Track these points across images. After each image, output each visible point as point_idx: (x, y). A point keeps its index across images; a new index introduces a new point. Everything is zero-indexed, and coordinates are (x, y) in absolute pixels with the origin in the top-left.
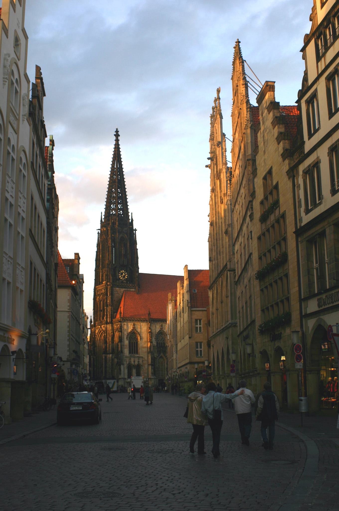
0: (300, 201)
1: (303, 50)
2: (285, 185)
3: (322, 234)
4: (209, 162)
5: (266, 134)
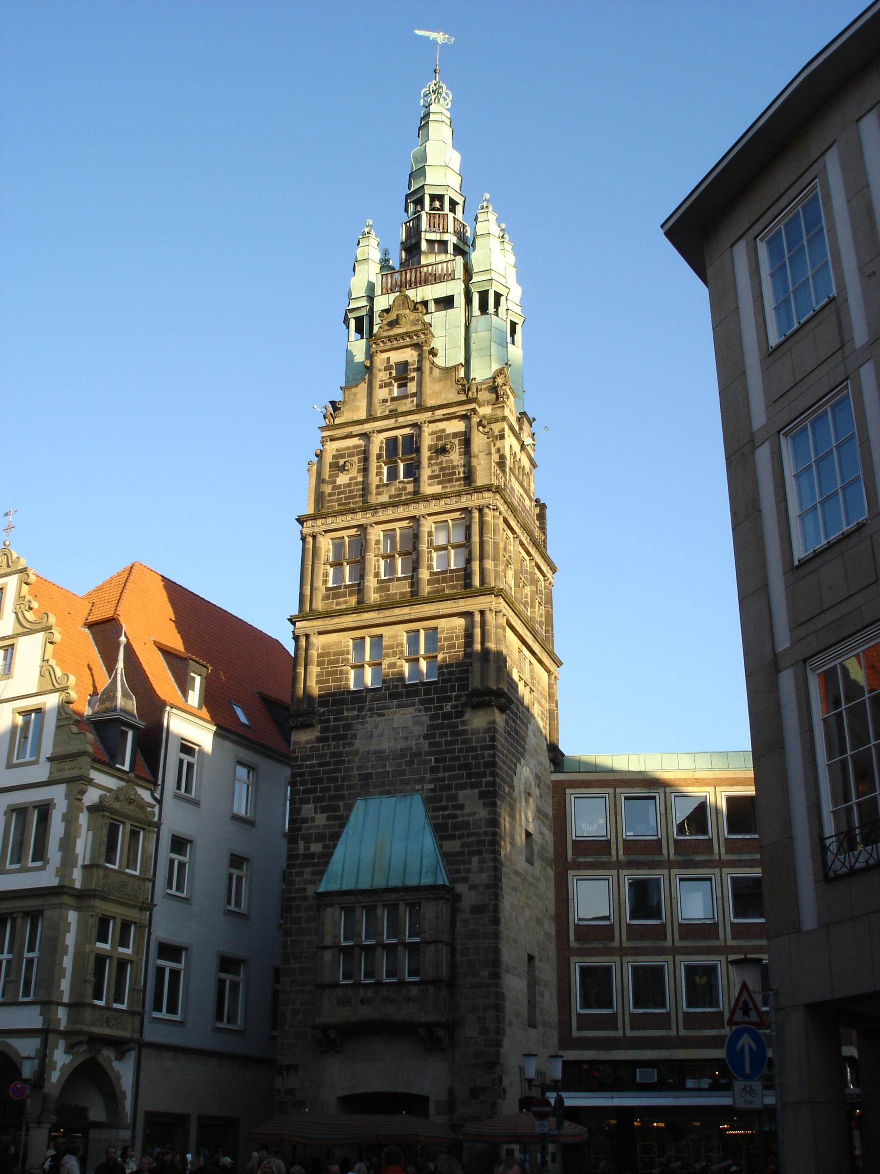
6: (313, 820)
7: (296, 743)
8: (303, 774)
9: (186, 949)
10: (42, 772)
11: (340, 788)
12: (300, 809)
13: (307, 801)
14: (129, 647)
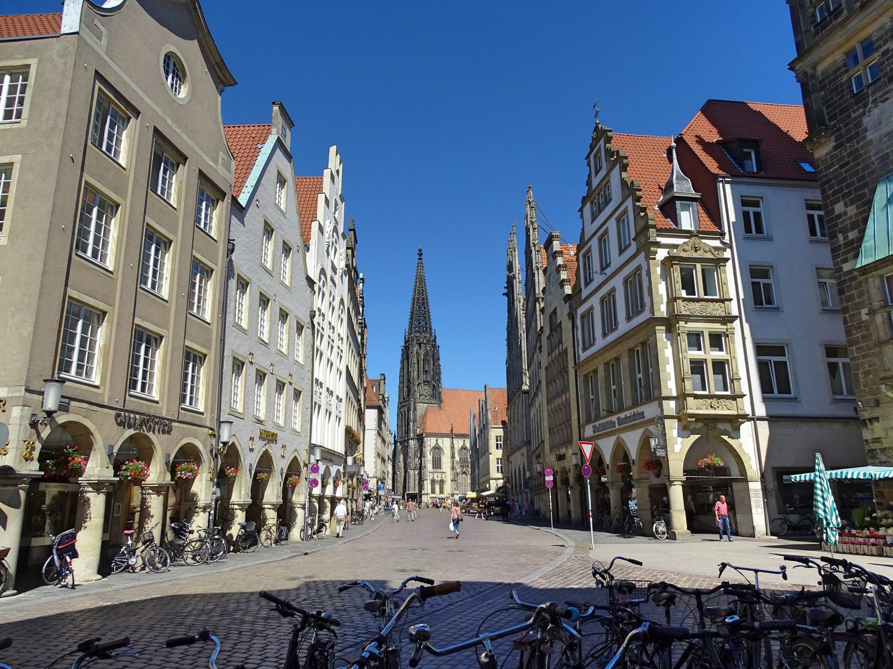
0: (578, 340)
1: (581, 210)
2: (567, 325)
3: (595, 371)
4: (506, 291)
6: (845, 213)
7: (819, 159)
8: (830, 180)
11: (863, 177)
12: (833, 209)
13: (837, 201)
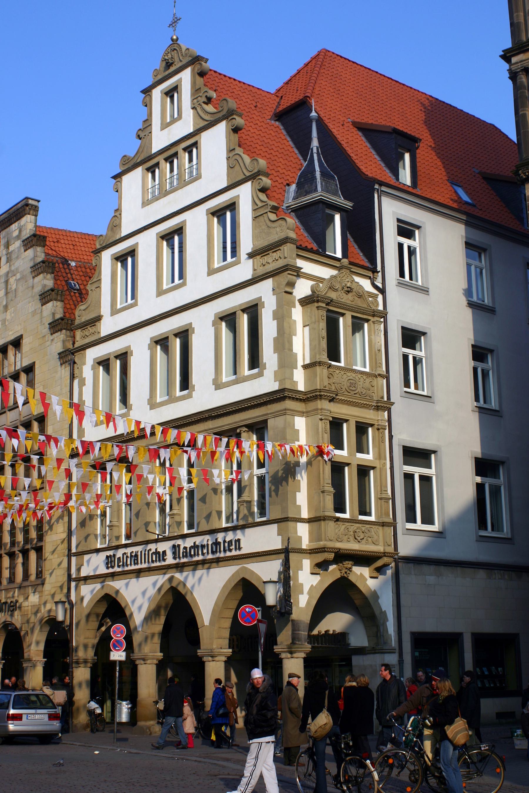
5: (12, 280)
9: (434, 452)
10: (244, 270)
14: (320, 121)
